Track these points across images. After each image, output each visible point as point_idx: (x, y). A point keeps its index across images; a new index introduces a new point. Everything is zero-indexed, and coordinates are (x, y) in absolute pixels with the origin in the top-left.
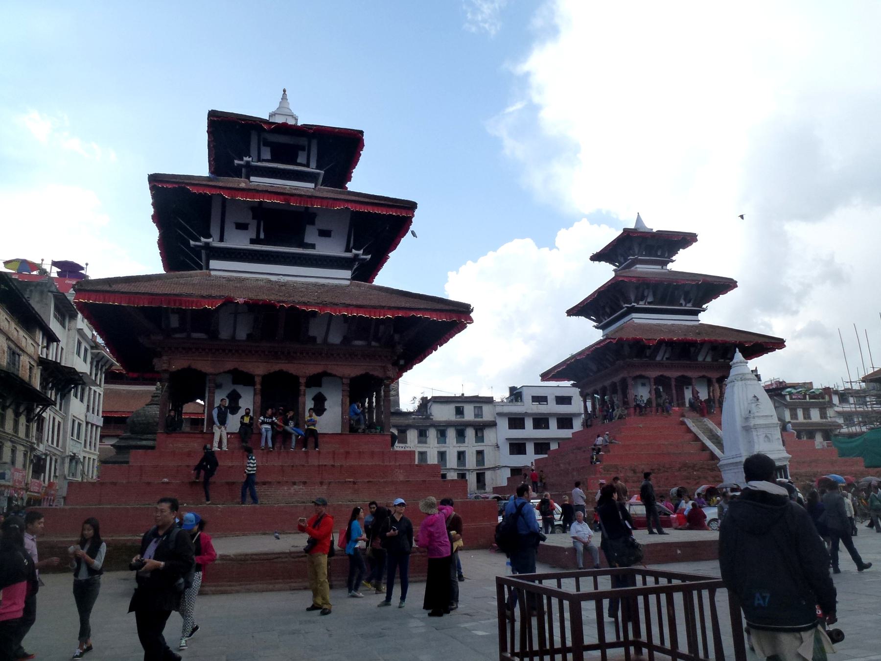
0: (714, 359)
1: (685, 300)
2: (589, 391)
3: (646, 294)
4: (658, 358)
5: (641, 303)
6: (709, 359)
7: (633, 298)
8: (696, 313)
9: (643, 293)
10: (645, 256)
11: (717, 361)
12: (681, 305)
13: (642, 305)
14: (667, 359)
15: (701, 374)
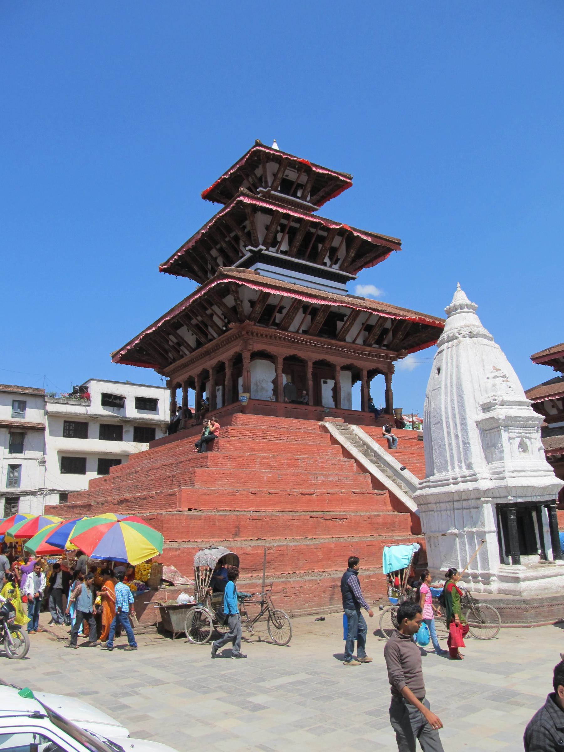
0: (365, 343)
1: (331, 258)
2: (182, 378)
3: (279, 240)
4: (292, 328)
5: (271, 249)
6: (360, 341)
7: (261, 240)
8: (343, 280)
9: (275, 238)
10: (280, 192)
11: (370, 345)
12: (325, 264)
13: (272, 252)
14: (304, 332)
15: (348, 361)
